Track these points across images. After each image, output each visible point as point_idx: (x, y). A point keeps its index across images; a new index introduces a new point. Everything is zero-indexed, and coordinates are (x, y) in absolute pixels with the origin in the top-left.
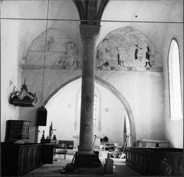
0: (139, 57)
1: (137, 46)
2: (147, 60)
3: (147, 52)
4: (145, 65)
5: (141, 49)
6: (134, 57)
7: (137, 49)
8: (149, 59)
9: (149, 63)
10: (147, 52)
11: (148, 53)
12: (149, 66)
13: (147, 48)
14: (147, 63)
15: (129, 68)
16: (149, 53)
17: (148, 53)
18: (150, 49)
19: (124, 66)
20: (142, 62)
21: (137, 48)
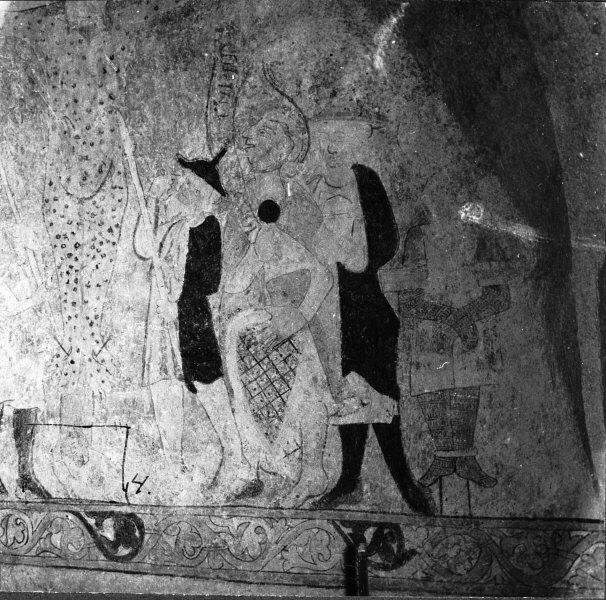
0: (246, 341)
1: (207, 170)
2: (361, 403)
3: (358, 263)
4: (335, 471)
5: (269, 212)
6: (166, 341)
7: (211, 223)
8: (384, 381)
9: (390, 435)
10: (358, 263)
11: (369, 277)
12: (393, 491)
13: (353, 193)
14: (352, 438)
15: (109, 533)
16: (389, 280)
17: (369, 277)
18: (401, 216)
19: (44, 495)
20: (288, 436)
21: (203, 203)
